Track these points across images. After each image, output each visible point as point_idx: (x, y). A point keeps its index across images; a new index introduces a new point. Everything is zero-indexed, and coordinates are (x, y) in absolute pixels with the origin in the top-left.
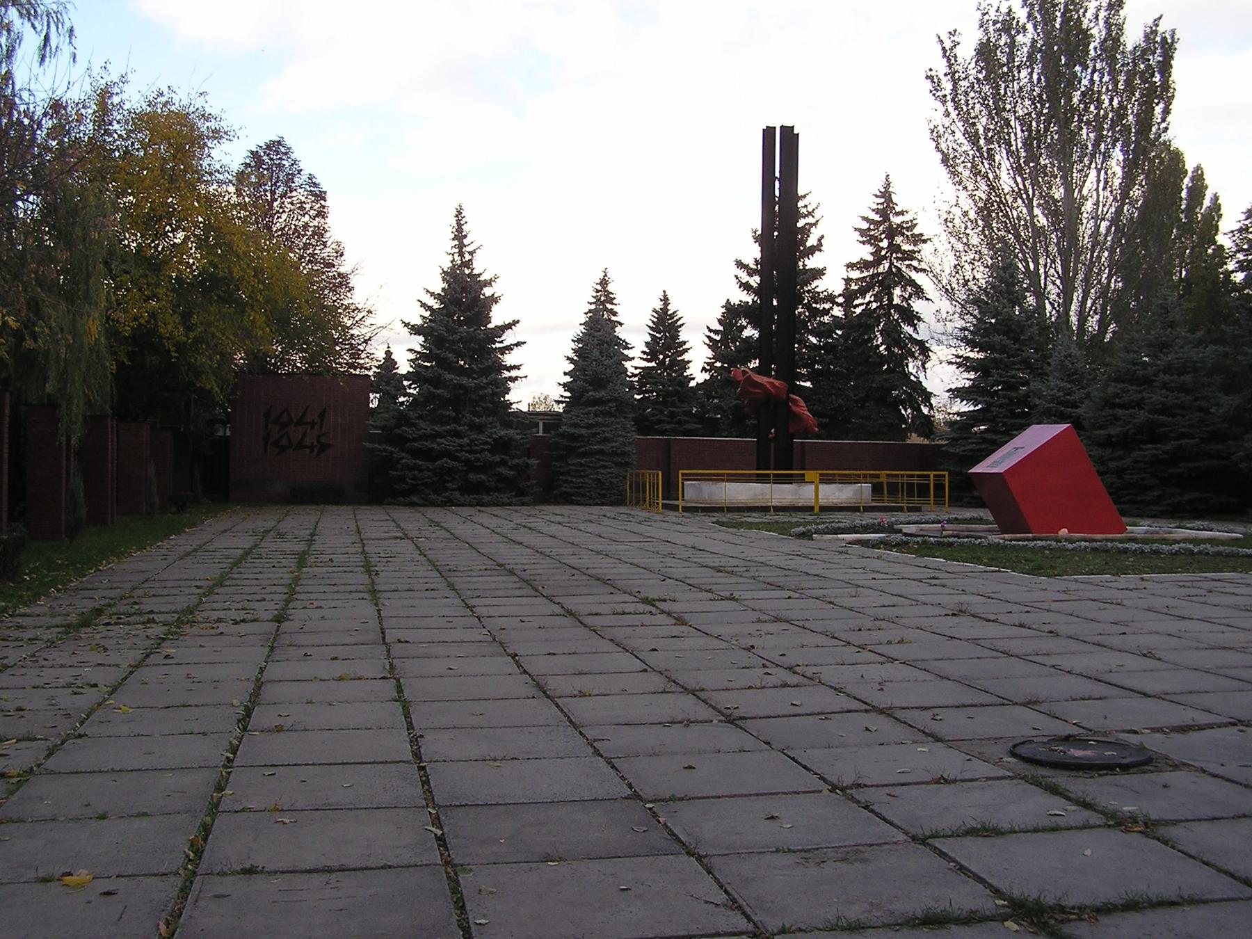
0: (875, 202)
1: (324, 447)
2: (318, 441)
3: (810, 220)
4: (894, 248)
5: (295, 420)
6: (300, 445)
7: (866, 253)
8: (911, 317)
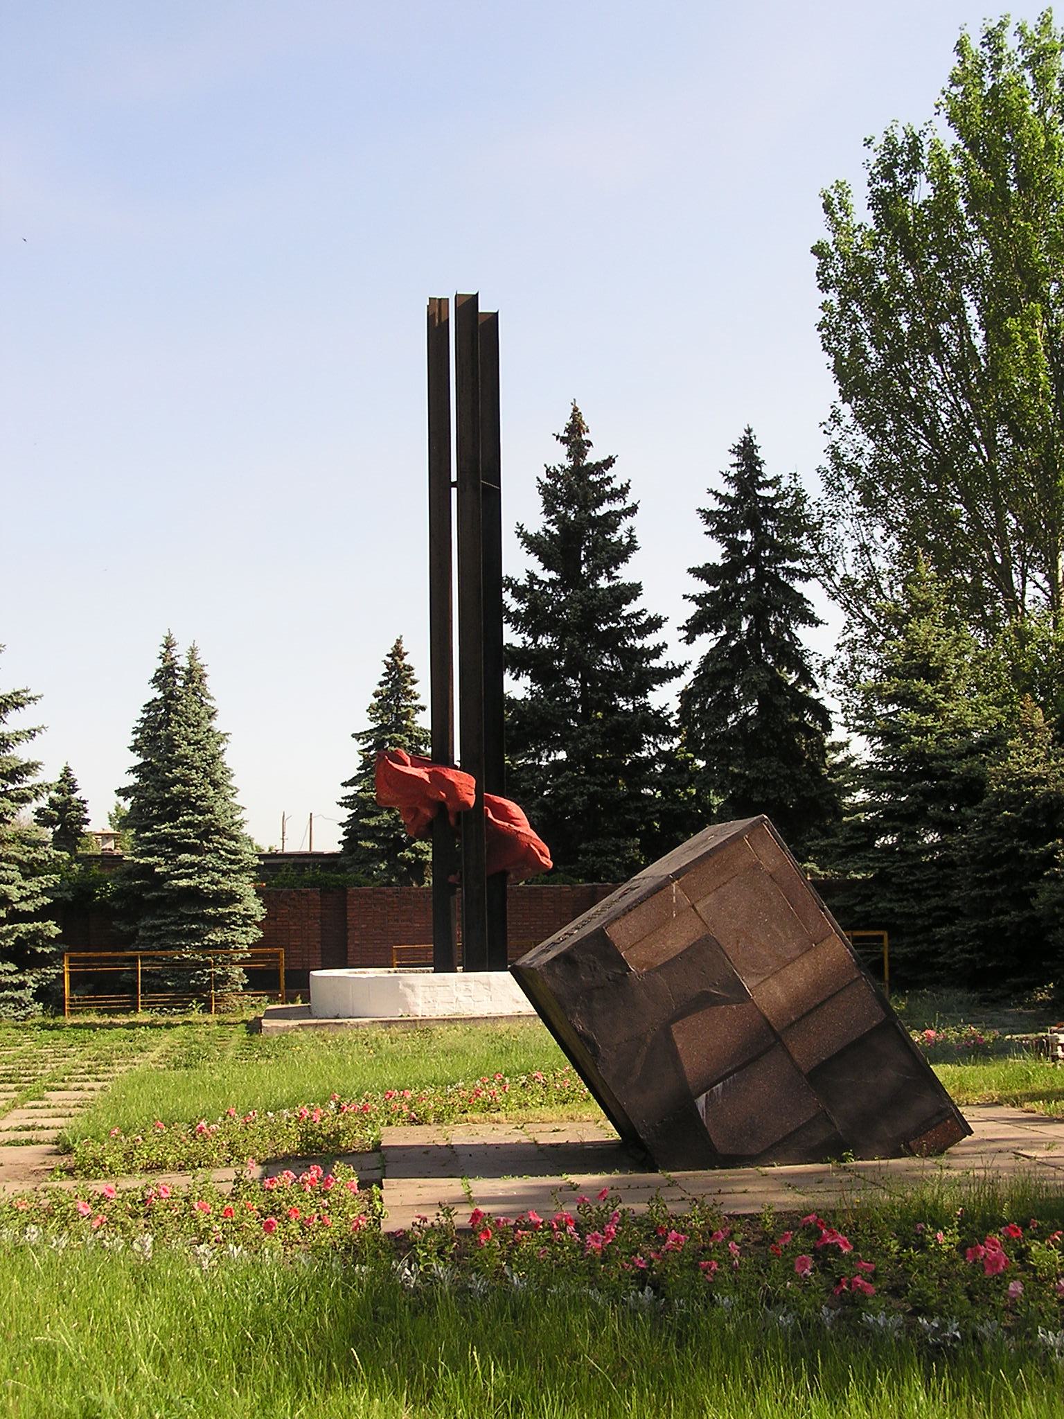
0: (728, 462)
3: (618, 506)
4: (762, 540)
7: (714, 553)
8: (793, 657)
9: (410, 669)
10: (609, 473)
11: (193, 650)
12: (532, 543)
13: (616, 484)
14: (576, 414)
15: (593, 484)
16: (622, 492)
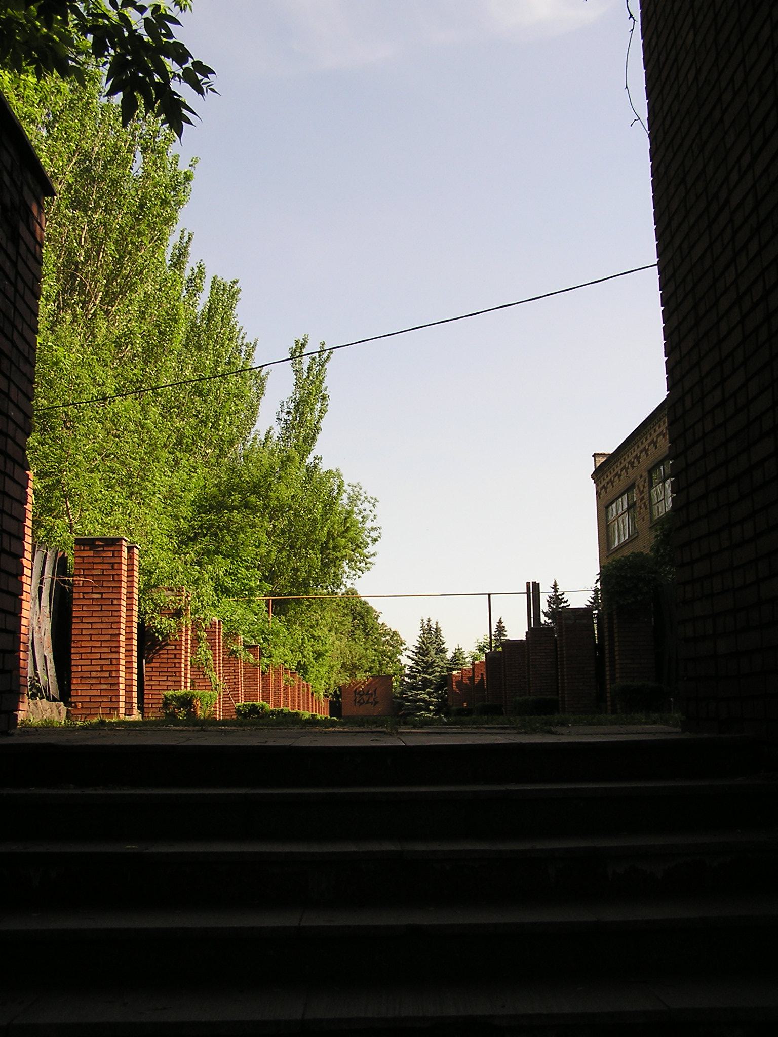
1: (376, 703)
2: (374, 700)
5: (365, 692)
6: (368, 702)
9: (504, 627)
10: (563, 596)
11: (437, 623)
12: (546, 614)
13: (565, 599)
14: (555, 582)
15: (559, 599)
16: (567, 601)
